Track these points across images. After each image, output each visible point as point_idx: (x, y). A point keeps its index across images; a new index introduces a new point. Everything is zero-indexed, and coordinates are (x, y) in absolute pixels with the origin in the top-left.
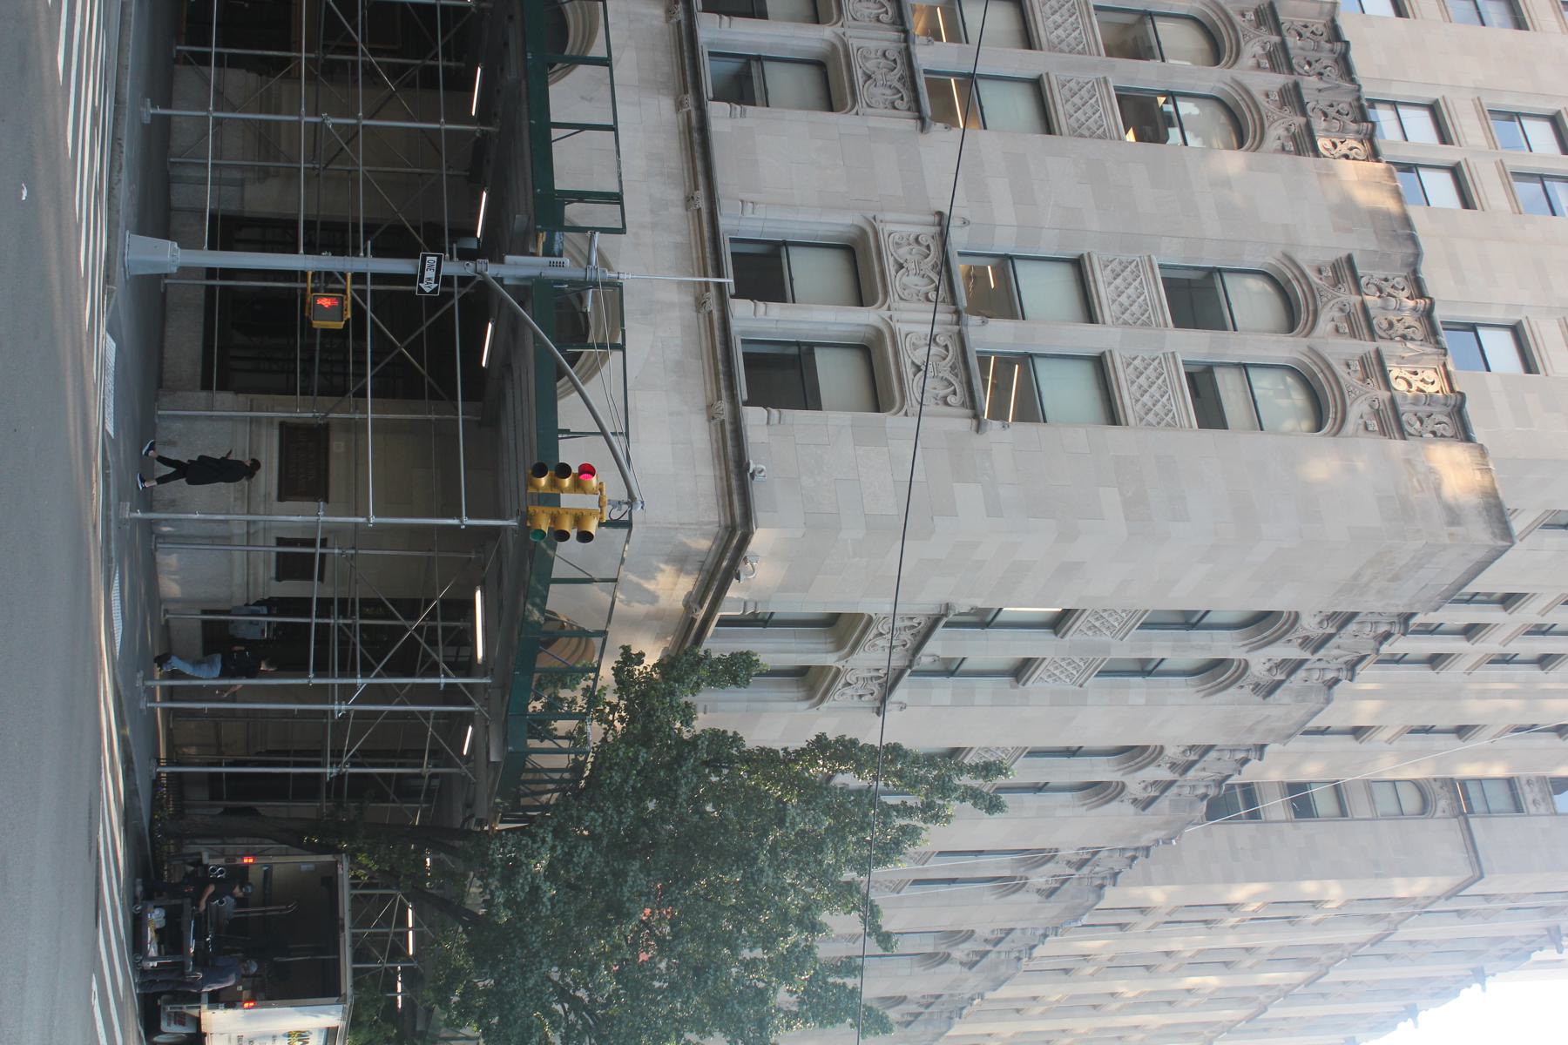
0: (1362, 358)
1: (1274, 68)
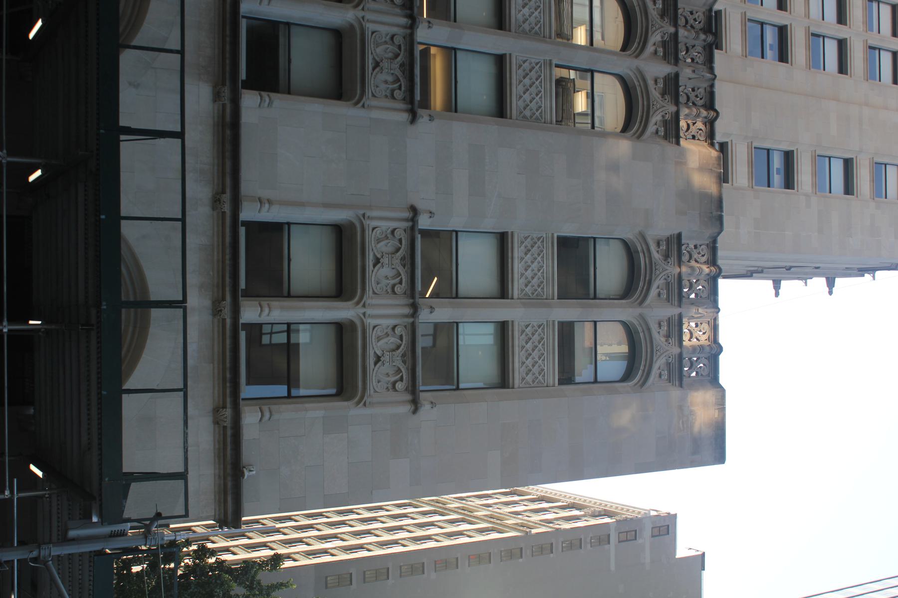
0: (669, 318)
1: (665, 57)
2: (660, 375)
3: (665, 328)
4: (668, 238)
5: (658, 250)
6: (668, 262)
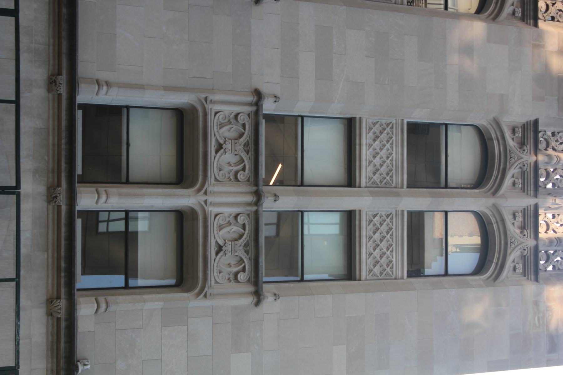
0: (524, 209)
2: (515, 269)
3: (520, 219)
4: (524, 125)
5: (513, 137)
6: (524, 150)
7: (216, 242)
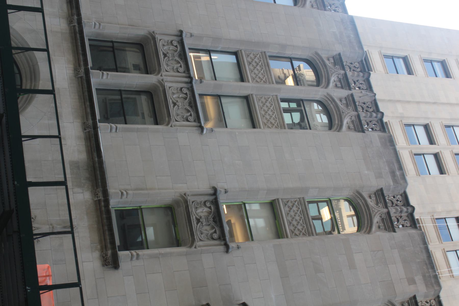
7: (172, 100)
